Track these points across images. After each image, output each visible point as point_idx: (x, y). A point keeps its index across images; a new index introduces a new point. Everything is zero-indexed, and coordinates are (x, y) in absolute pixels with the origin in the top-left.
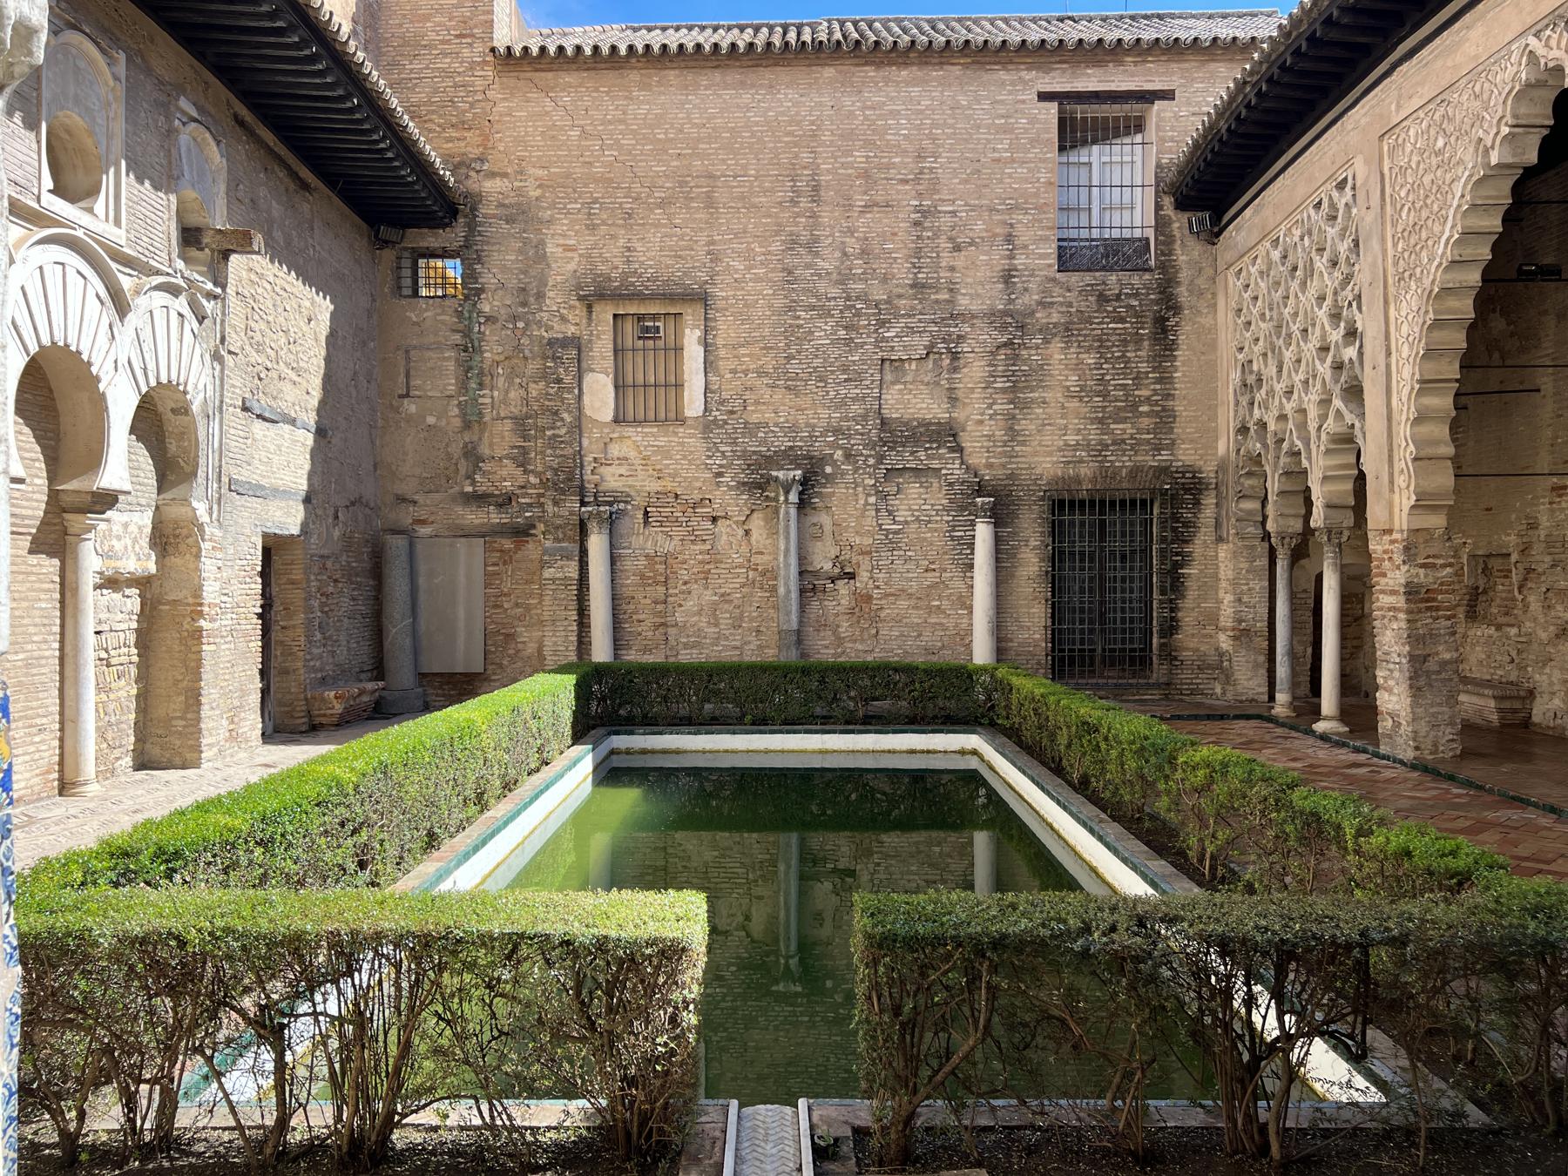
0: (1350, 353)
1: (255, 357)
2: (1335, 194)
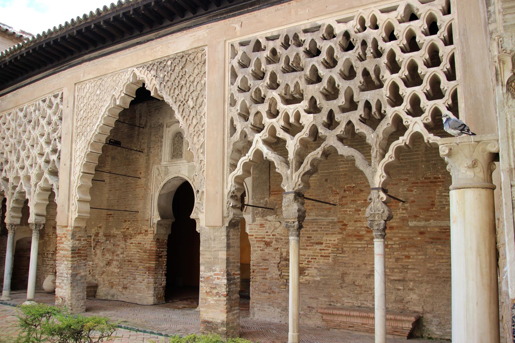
0: (54, 157)
2: (53, 99)
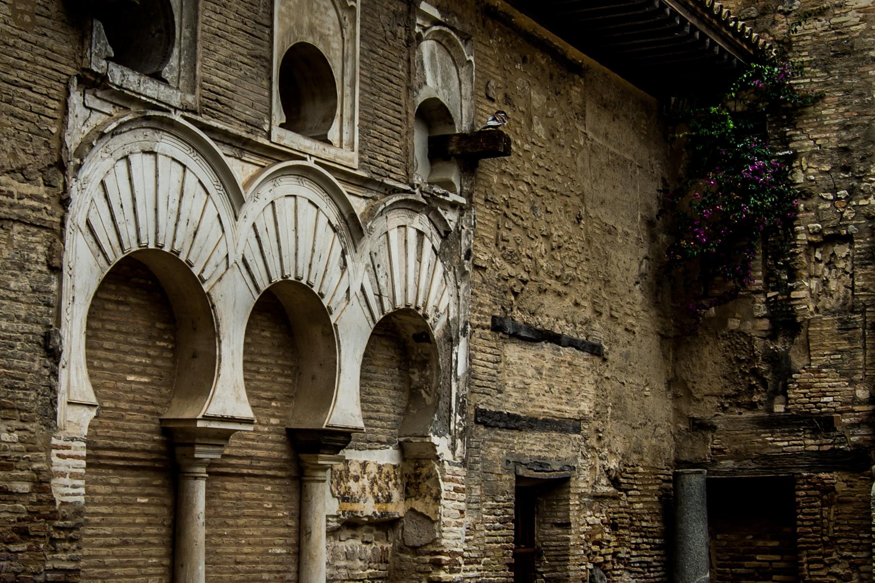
1: (509, 269)
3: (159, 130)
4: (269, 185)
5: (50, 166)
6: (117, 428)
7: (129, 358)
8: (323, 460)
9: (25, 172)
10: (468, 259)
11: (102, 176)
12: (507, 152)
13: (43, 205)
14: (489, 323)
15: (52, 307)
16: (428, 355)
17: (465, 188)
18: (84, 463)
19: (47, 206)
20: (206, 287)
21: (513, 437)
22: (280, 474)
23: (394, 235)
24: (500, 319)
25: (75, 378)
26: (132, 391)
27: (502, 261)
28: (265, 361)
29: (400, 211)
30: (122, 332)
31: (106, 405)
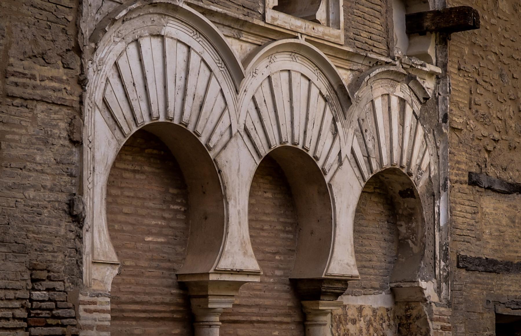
1: (482, 131)
3: (165, 15)
4: (265, 62)
5: (68, 50)
6: (138, 284)
7: (146, 221)
8: (324, 305)
9: (45, 57)
10: (446, 122)
11: (115, 59)
12: (476, 26)
13: (63, 86)
14: (466, 178)
15: (75, 177)
16: (413, 209)
17: (440, 59)
18: (109, 316)
19: (66, 86)
20: (212, 154)
21: (492, 279)
22: (286, 320)
23: (379, 103)
24: (476, 174)
25: (98, 239)
26: (150, 251)
27: (476, 123)
28: (268, 219)
29: (383, 81)
30: (139, 198)
31: (128, 263)
